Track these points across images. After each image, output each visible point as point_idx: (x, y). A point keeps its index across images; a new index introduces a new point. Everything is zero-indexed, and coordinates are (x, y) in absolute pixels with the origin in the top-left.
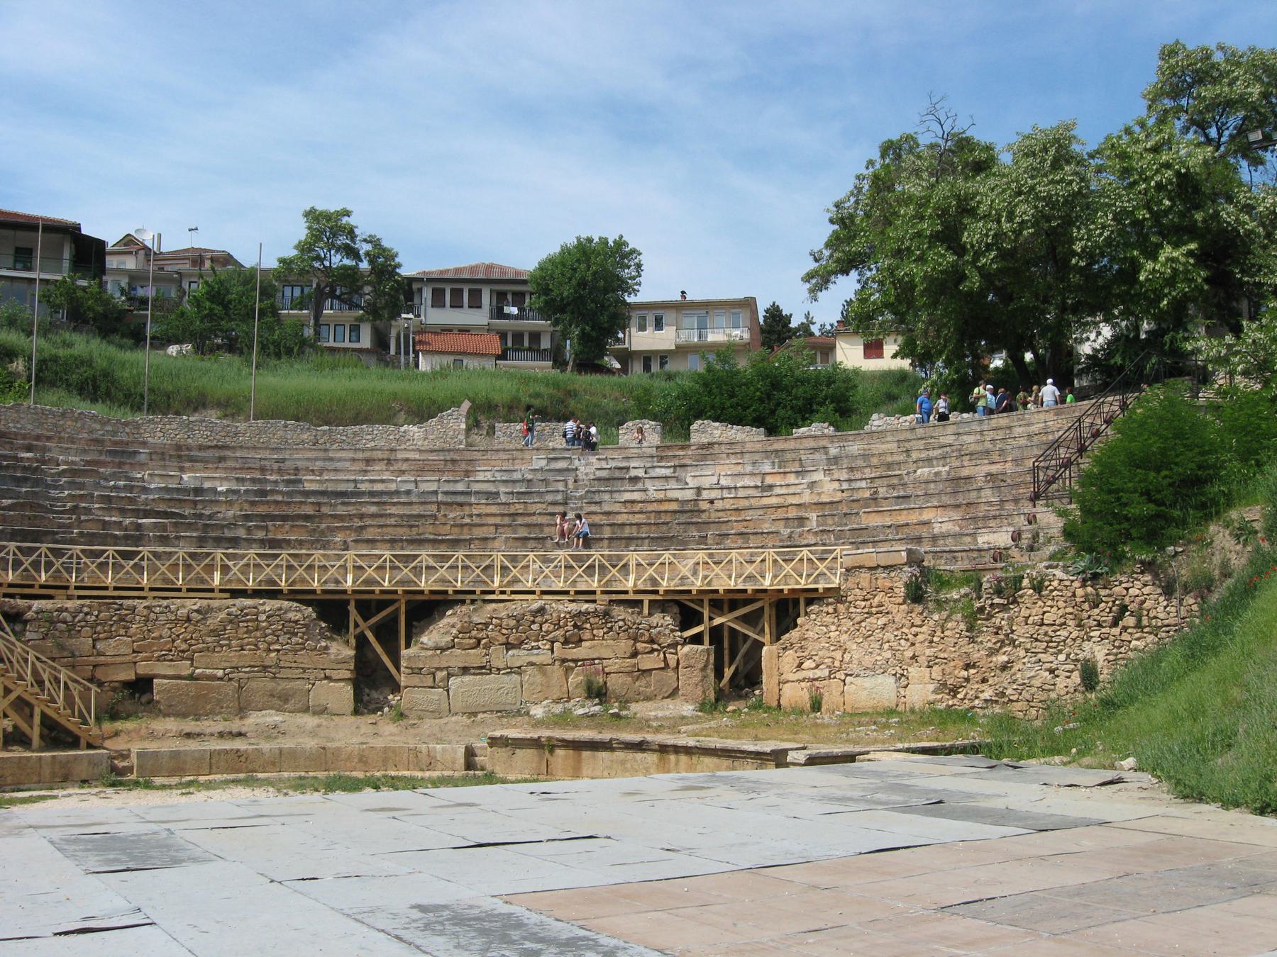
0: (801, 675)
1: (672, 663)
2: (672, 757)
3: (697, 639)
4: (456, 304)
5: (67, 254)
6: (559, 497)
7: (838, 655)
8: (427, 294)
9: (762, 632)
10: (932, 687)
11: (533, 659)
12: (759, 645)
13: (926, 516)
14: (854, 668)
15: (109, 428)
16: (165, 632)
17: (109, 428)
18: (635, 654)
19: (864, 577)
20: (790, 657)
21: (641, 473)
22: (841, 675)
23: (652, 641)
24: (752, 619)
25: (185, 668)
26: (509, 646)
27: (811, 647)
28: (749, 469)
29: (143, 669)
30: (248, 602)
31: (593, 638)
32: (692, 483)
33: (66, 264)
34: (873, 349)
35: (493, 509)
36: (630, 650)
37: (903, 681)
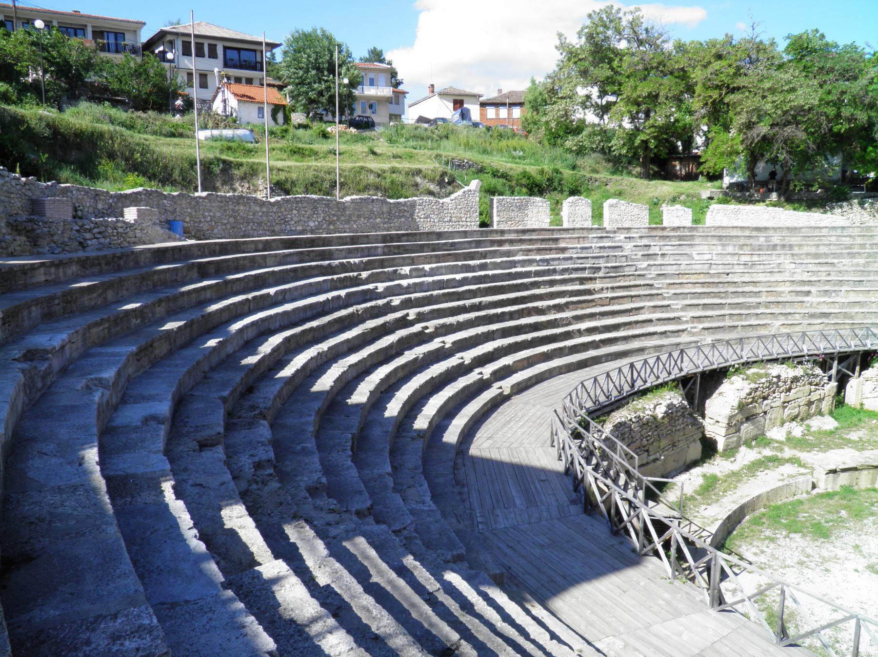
4: (200, 54)
15: (264, 210)
17: (264, 210)
18: (811, 392)
23: (816, 385)
26: (765, 398)
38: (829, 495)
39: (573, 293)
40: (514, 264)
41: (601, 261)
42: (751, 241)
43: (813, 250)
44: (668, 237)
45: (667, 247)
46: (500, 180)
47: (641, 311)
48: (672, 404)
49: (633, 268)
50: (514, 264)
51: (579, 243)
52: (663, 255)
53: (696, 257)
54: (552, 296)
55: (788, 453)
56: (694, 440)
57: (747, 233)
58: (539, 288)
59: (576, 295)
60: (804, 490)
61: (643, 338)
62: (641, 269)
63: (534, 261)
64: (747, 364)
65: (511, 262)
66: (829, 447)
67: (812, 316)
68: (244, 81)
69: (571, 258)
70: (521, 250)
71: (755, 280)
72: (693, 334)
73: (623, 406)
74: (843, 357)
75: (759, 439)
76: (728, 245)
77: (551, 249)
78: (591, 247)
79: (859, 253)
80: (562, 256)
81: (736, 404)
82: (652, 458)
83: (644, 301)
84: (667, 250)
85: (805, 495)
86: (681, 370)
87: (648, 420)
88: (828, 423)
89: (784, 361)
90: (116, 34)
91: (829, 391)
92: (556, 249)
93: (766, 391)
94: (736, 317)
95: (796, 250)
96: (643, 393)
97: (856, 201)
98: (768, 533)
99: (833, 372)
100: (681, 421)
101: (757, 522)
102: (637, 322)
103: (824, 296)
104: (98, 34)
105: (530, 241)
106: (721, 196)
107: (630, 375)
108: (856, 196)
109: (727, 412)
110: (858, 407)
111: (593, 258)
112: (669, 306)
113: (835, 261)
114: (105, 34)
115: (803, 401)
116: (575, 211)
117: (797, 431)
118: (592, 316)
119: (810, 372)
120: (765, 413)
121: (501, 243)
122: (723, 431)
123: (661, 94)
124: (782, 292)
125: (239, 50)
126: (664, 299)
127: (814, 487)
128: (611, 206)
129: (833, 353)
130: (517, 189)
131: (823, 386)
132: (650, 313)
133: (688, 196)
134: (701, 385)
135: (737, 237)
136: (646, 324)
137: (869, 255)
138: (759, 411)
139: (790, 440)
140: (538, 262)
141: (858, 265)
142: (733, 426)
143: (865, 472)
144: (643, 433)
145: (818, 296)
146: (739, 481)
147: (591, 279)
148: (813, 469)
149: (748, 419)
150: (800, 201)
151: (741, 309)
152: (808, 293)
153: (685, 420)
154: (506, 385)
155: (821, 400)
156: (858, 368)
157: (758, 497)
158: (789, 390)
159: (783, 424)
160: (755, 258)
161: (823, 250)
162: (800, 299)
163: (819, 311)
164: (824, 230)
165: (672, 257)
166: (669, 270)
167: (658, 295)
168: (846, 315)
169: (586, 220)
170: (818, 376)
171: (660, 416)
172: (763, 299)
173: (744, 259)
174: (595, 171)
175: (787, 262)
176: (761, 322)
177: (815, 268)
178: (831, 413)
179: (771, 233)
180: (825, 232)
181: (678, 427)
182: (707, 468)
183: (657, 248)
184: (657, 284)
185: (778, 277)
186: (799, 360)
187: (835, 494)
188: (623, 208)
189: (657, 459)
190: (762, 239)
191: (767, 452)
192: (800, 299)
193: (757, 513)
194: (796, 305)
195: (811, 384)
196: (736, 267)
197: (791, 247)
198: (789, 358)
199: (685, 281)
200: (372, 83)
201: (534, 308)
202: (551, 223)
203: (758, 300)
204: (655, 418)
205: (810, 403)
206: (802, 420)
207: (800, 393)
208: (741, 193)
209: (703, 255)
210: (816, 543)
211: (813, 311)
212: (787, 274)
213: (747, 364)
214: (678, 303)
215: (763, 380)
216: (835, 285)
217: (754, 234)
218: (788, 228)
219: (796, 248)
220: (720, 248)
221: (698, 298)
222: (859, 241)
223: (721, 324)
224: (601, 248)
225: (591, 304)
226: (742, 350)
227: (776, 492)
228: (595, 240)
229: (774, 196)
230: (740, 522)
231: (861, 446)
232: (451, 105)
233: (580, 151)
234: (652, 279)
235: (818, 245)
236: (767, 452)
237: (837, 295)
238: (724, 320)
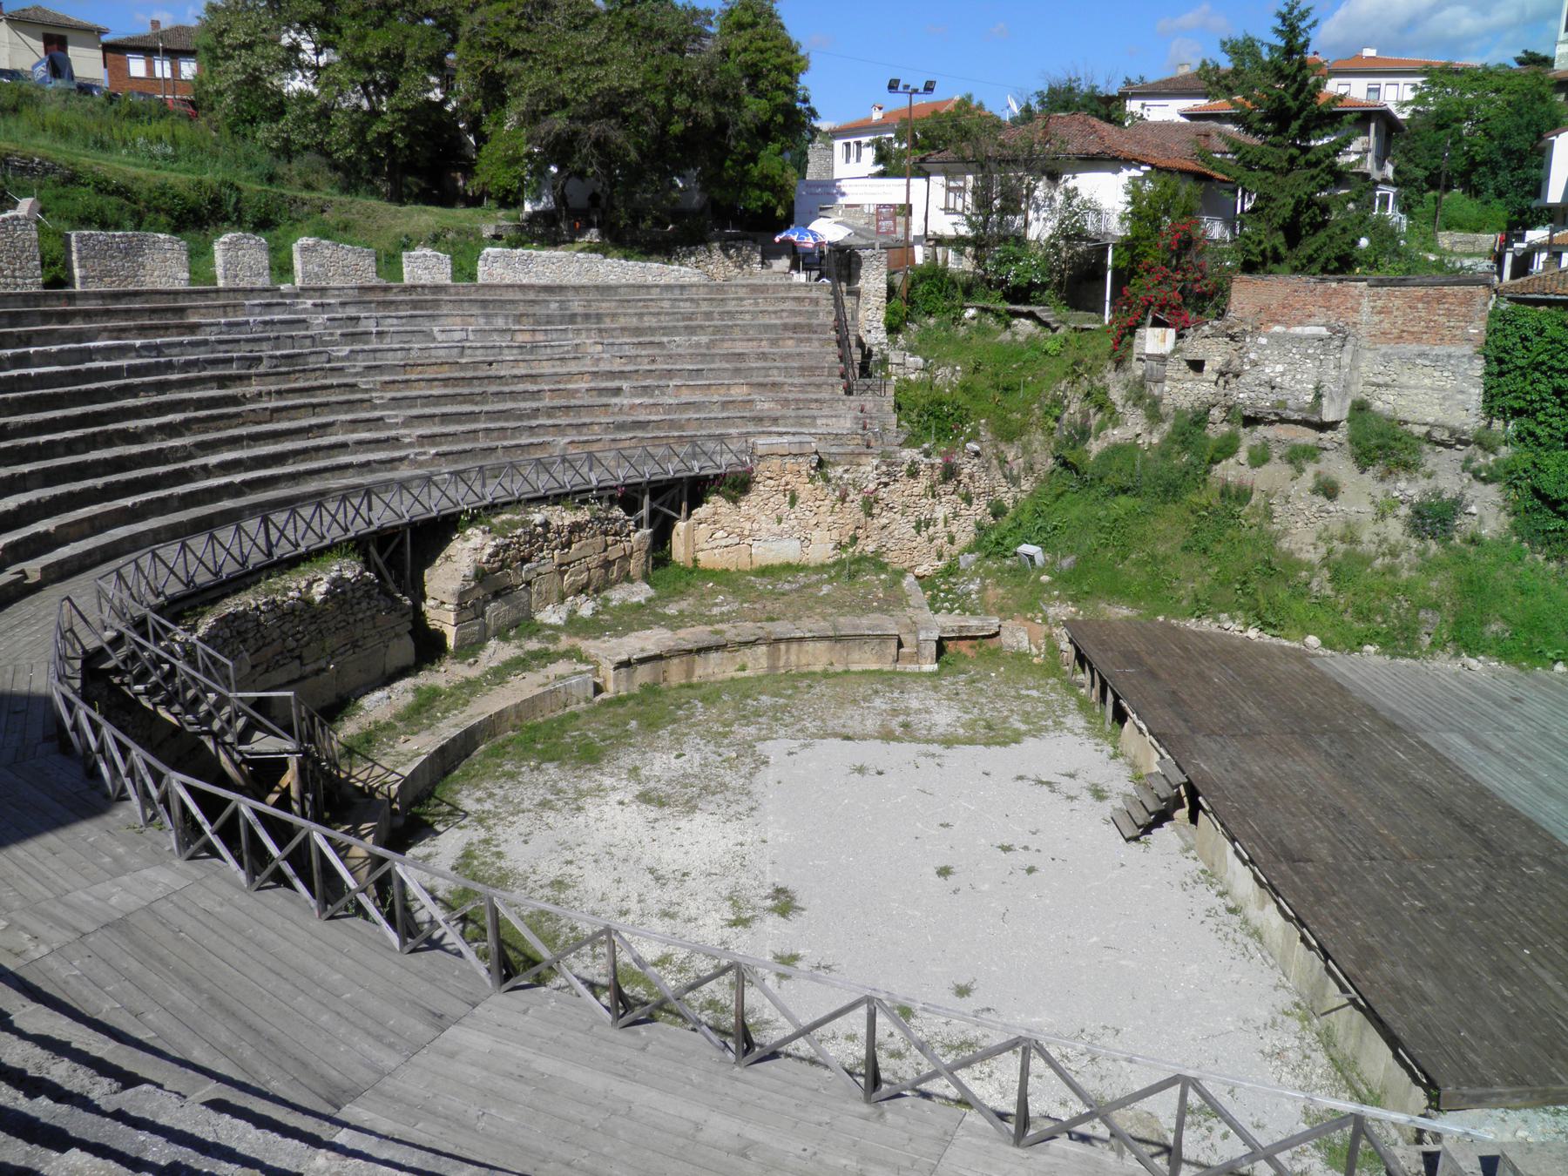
3: (639, 525)
7: (748, 525)
10: (832, 546)
18: (607, 546)
19: (775, 462)
22: (749, 541)
23: (615, 534)
26: (525, 560)
27: (725, 521)
37: (806, 543)
38: (620, 701)
39: (200, 404)
40: (89, 355)
41: (264, 346)
42: (537, 309)
43: (634, 322)
44: (392, 302)
45: (390, 321)
46: (113, 199)
47: (329, 430)
48: (341, 578)
49: (324, 358)
50: (89, 355)
51: (226, 315)
52: (379, 333)
53: (440, 337)
54: (159, 409)
55: (565, 642)
56: (397, 636)
57: (531, 296)
58: (136, 396)
59: (208, 407)
60: (582, 696)
61: (328, 475)
62: (339, 359)
63: (132, 348)
64: (494, 508)
65: (81, 350)
66: (629, 629)
67: (621, 427)
69: (205, 343)
70: (105, 329)
71: (534, 372)
72: (421, 465)
73: (247, 587)
74: (659, 489)
75: (523, 625)
76: (496, 315)
77: (167, 327)
78: (247, 323)
79: (701, 327)
80: (186, 339)
81: (469, 572)
82: (309, 668)
83: (338, 413)
84: (390, 325)
85: (583, 705)
86: (370, 523)
87: (293, 609)
88: (640, 592)
89: (557, 499)
91: (639, 543)
92: (178, 326)
93: (526, 550)
94: (495, 434)
95: (607, 323)
96: (292, 563)
97: (717, 245)
98: (508, 767)
100: (364, 605)
101: (499, 752)
102: (318, 449)
103: (641, 396)
105: (127, 313)
106: (512, 234)
107: (262, 534)
108: (718, 239)
109: (455, 585)
110: (691, 565)
111: (248, 341)
112: (381, 419)
113: (665, 339)
115: (595, 560)
116: (235, 256)
117: (586, 609)
118: (234, 442)
119: (603, 515)
120: (529, 583)
121: (64, 317)
122: (452, 617)
123: (408, 52)
124: (577, 391)
126: (375, 407)
127: (598, 689)
128: (304, 249)
129: (640, 484)
130: (150, 217)
132: (346, 432)
133: (459, 233)
134: (407, 549)
135: (512, 302)
136: (336, 452)
137: (717, 330)
138: (513, 580)
139: (575, 625)
140: (138, 352)
141: (698, 345)
142: (468, 606)
143: (676, 661)
144: (286, 628)
145: (633, 396)
146: (472, 694)
147: (240, 378)
148: (597, 664)
149: (497, 595)
150: (635, 243)
151: (506, 420)
152: (618, 391)
153: (374, 603)
154: (33, 568)
155: (626, 557)
156: (684, 505)
157: (500, 714)
158: (568, 544)
159: (562, 599)
160: (540, 337)
161: (649, 321)
162: (605, 400)
163: (630, 419)
164: (654, 291)
165: (397, 338)
166: (390, 359)
167: (362, 401)
168: (672, 424)
169: (260, 275)
170: (616, 520)
171: (318, 598)
172: (547, 402)
173: (520, 338)
174: (308, 186)
175: (590, 343)
176: (535, 440)
177: (634, 352)
178: (646, 578)
179: (570, 295)
180: (655, 294)
181: (360, 616)
182: (425, 679)
183: (372, 322)
184: (362, 382)
185: (573, 367)
186: (583, 496)
187: (631, 697)
188: (327, 253)
189: (324, 670)
190: (554, 306)
191: (533, 645)
192: (605, 400)
193: (500, 739)
194: (597, 411)
195: (606, 533)
196: (506, 351)
197: (599, 317)
198: (567, 494)
199: (413, 377)
201: (117, 431)
202: (191, 281)
203: (535, 405)
204: (309, 603)
205: (607, 564)
206: (597, 591)
207: (587, 550)
208: (547, 231)
209: (451, 332)
210: (578, 773)
211: (620, 419)
212: (588, 361)
213: (494, 508)
214: (396, 415)
215: (519, 531)
216: (661, 377)
217: (543, 296)
218: (597, 287)
219: (608, 320)
220: (482, 321)
221: (434, 405)
222: (705, 307)
223: (468, 446)
224: (265, 323)
225: (235, 421)
226: (484, 485)
227: (532, 704)
228: (257, 310)
229: (593, 235)
230: (467, 756)
231: (674, 623)
233: (286, 151)
234: (356, 374)
235: (641, 315)
236: (533, 645)
237: (663, 394)
238: (476, 440)
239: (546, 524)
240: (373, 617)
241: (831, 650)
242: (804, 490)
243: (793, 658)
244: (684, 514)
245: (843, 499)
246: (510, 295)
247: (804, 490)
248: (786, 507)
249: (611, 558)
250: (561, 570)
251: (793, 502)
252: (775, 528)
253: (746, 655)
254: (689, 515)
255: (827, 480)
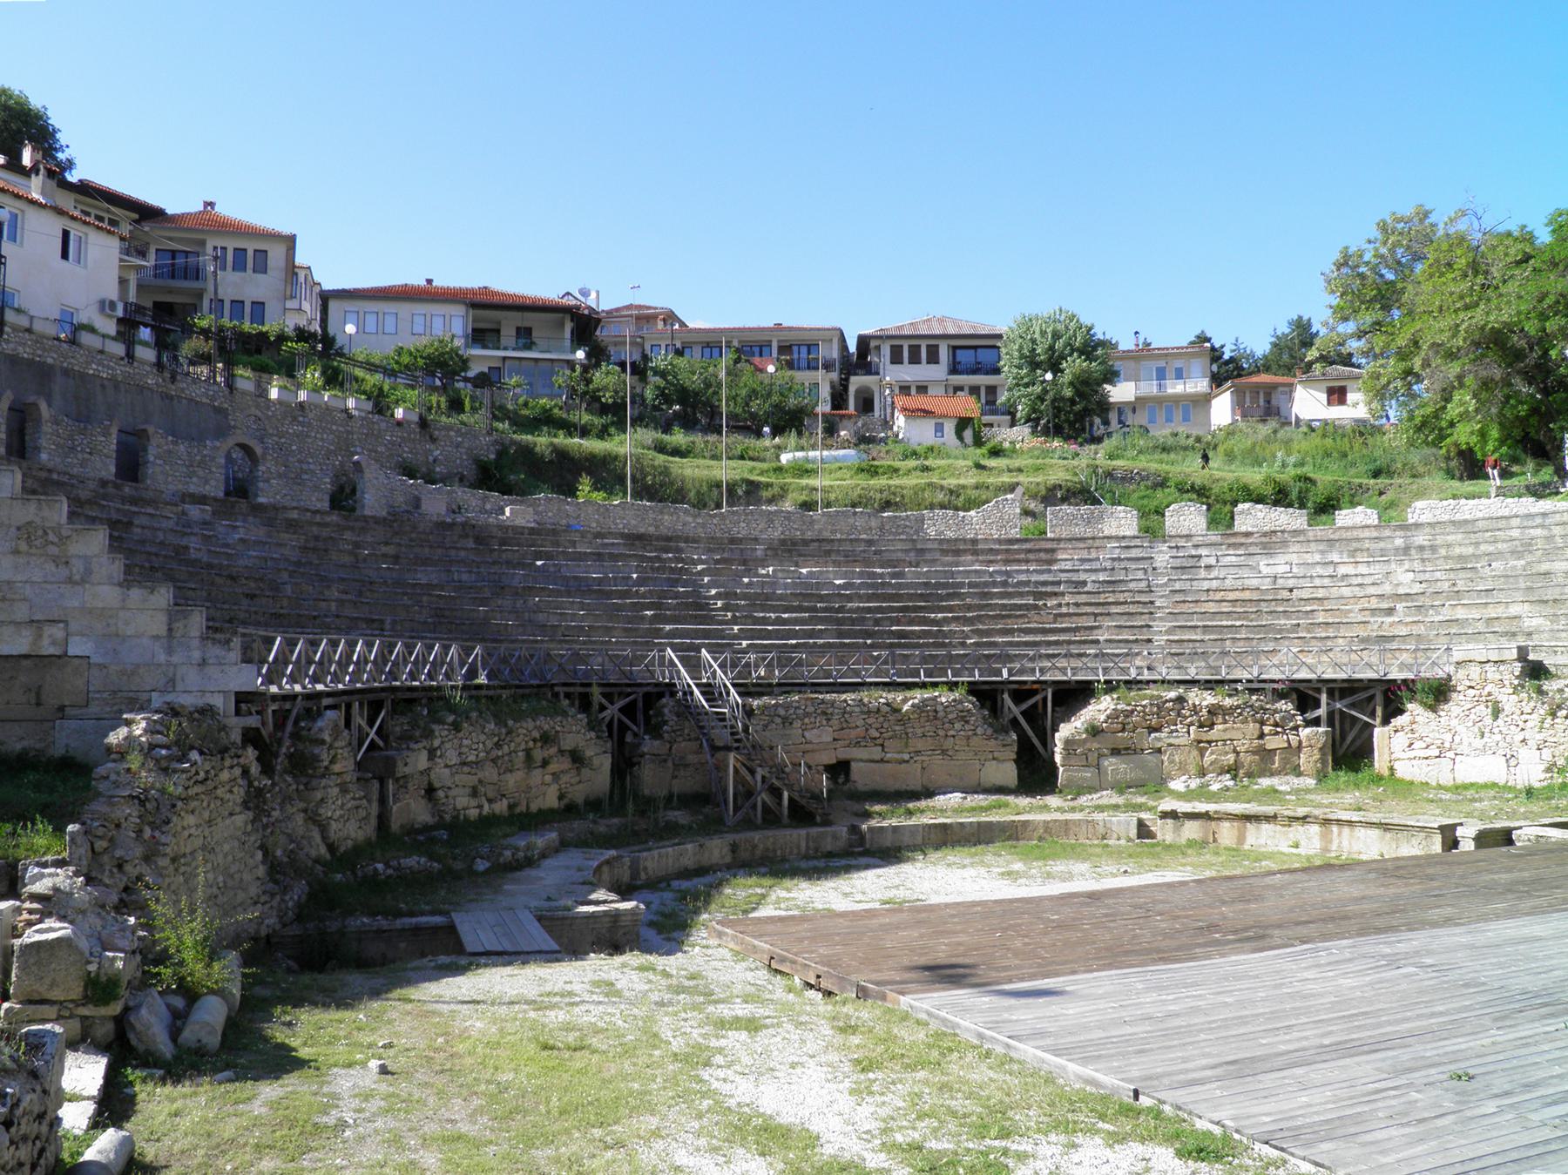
0: (1412, 754)
1: (1294, 744)
2: (1335, 829)
3: (1316, 722)
4: (915, 359)
5: (568, 334)
6: (1143, 585)
8: (886, 350)
9: (1373, 715)
11: (1172, 741)
12: (1370, 727)
13: (1514, 610)
14: (1464, 748)
16: (860, 723)
18: (1262, 736)
19: (1475, 671)
20: (1400, 740)
21: (1212, 561)
22: (1451, 754)
23: (1276, 725)
24: (1366, 705)
25: (876, 753)
27: (1421, 730)
28: (1317, 557)
29: (844, 754)
30: (928, 694)
31: (1225, 722)
32: (1265, 570)
33: (568, 343)
34: (1337, 395)
35: (1082, 599)
36: (1257, 733)
37: (1513, 762)
68: (913, 391)
74: (1346, 689)
85: (1123, 842)
89: (1209, 685)
90: (809, 346)
99: (1322, 712)
100: (958, 726)
104: (785, 349)
110: (1386, 773)
114: (795, 349)
124: (1350, 611)
125: (975, 348)
131: (1296, 728)
143: (1226, 824)
149: (1116, 752)
152: (1390, 611)
173: (1342, 570)
197: (1433, 548)
200: (1179, 375)
232: (1324, 397)
239: (1180, 700)
240: (968, 738)
241: (1383, 839)
242: (1509, 702)
243: (1345, 843)
244: (1378, 720)
245: (1553, 715)
246: (1355, 533)
247: (1509, 702)
248: (1488, 720)
249: (1268, 747)
250: (1201, 746)
251: (1497, 712)
252: (1478, 743)
253: (1298, 831)
254: (1386, 722)
255: (1540, 692)
